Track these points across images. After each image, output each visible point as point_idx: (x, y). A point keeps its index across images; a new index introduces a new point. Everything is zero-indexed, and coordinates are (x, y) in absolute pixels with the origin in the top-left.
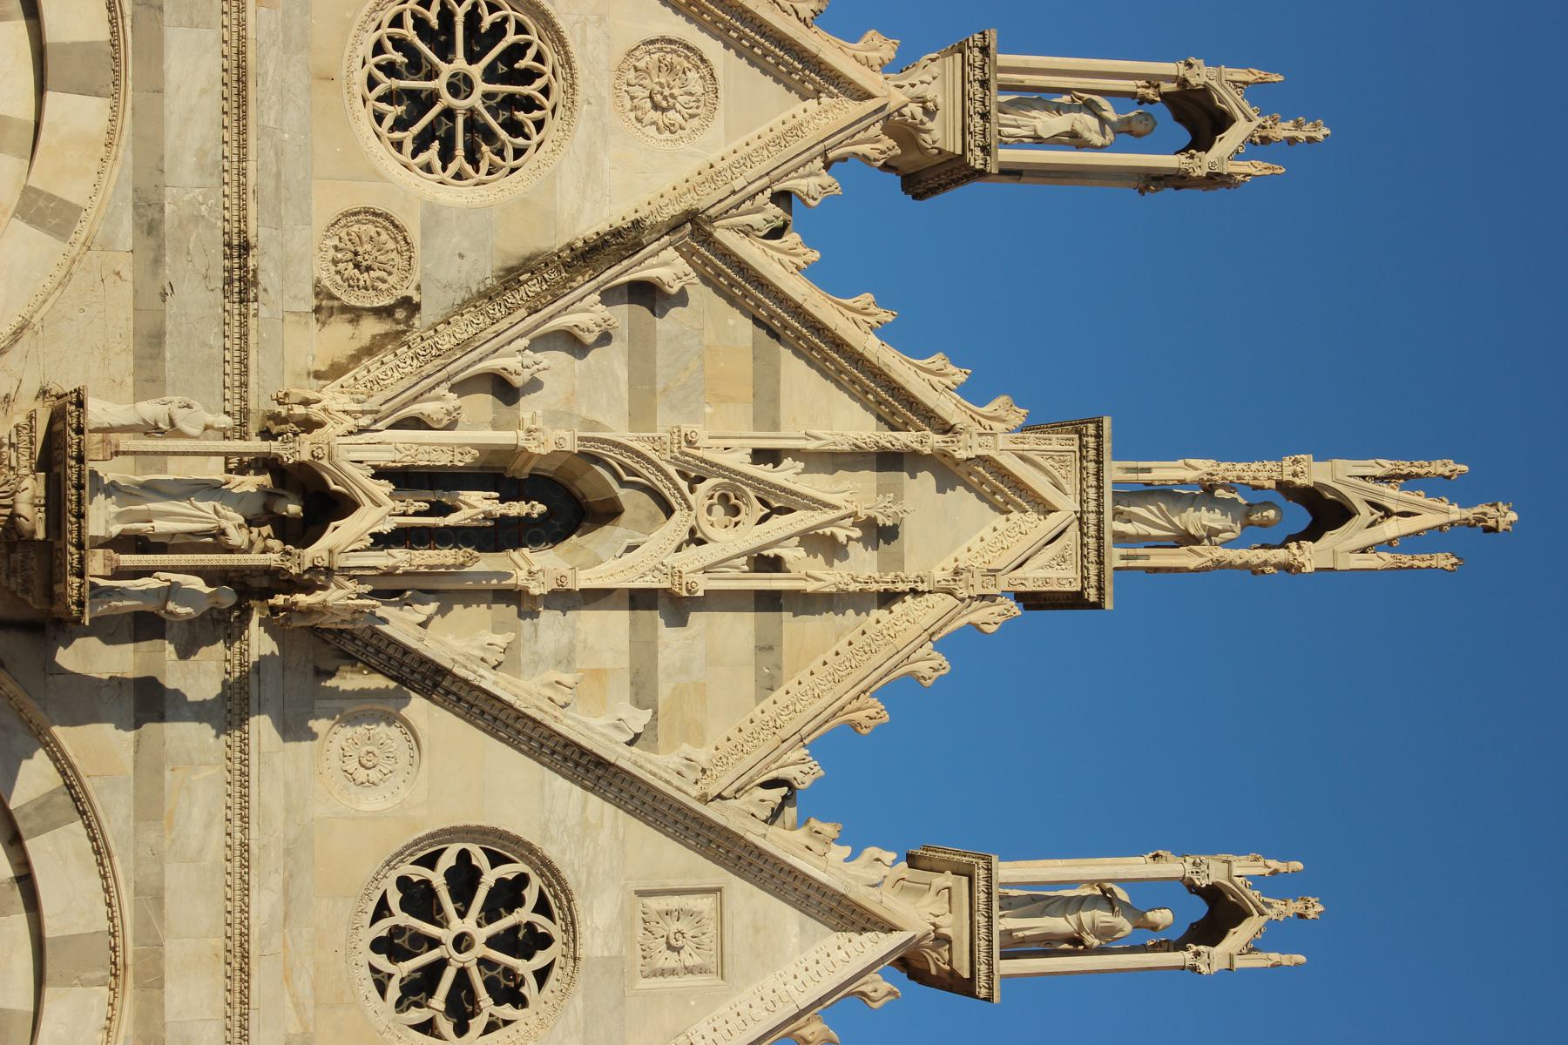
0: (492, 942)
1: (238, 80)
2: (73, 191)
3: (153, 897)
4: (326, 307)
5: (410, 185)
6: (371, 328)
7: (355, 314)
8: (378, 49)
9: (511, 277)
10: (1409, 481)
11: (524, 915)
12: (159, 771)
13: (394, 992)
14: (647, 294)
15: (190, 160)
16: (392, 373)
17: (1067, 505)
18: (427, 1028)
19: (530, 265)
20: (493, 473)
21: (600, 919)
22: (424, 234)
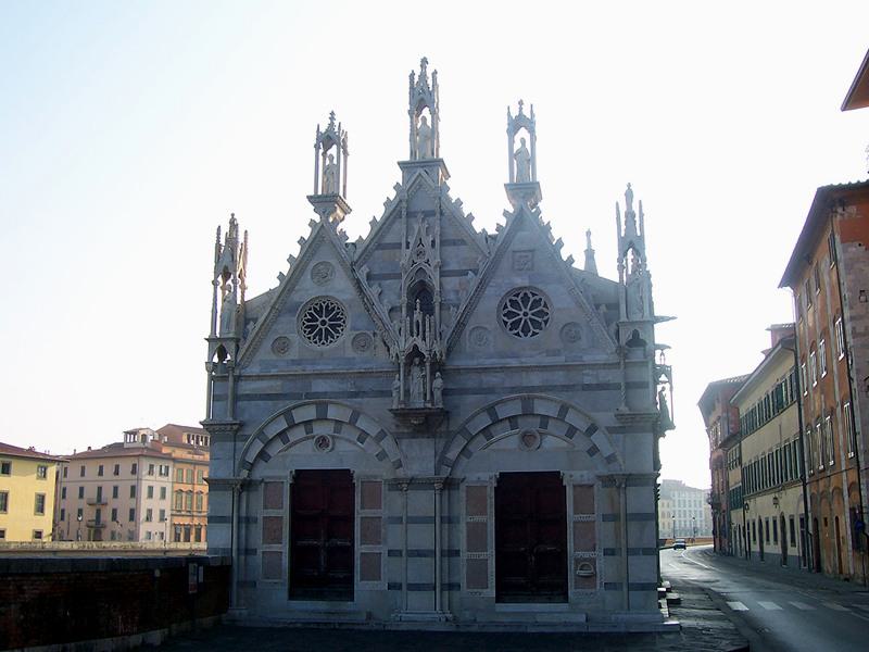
0: (526, 308)
2: (349, 412)
3: (513, 390)
5: (346, 336)
8: (316, 342)
11: (519, 299)
12: (484, 389)
13: (537, 331)
15: (341, 386)
18: (546, 322)
20: (411, 309)
22: (358, 330)
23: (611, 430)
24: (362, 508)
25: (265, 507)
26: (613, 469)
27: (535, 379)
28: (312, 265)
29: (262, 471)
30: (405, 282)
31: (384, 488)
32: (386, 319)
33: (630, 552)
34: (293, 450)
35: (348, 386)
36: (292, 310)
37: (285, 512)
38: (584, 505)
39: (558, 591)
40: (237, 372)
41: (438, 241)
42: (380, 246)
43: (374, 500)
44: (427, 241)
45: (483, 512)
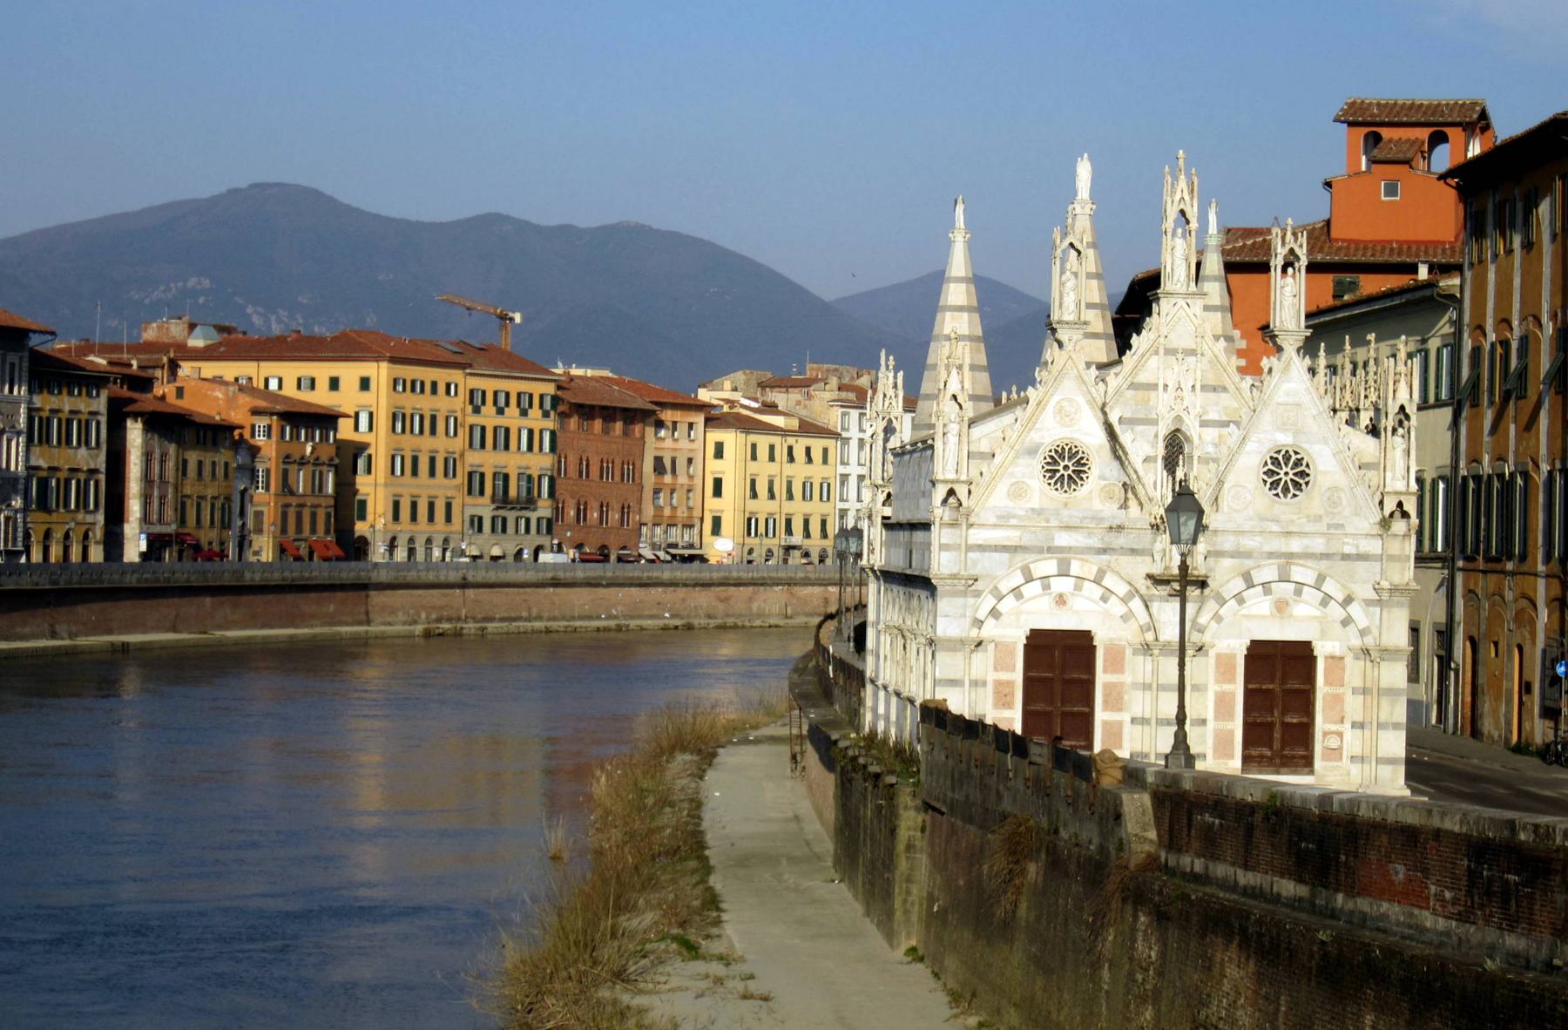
1: (1068, 528)
2: (1095, 569)
3: (1271, 555)
4: (1124, 506)
6: (1130, 494)
7: (1126, 499)
9: (1118, 458)
10: (1173, 193)
14: (1121, 420)
16: (1140, 489)
17: (1181, 302)
19: (1114, 451)
21: (1285, 439)
23: (1369, 603)
24: (1105, 671)
25: (996, 669)
26: (1369, 641)
27: (1295, 545)
28: (1056, 398)
29: (990, 630)
30: (1164, 430)
31: (1129, 652)
32: (1141, 473)
33: (1380, 726)
34: (1027, 606)
35: (1095, 542)
36: (1032, 451)
37: (1017, 676)
38: (1335, 679)
39: (1307, 763)
40: (972, 520)
41: (1198, 387)
42: (1133, 386)
43: (1116, 664)
44: (1187, 386)
45: (1232, 680)
